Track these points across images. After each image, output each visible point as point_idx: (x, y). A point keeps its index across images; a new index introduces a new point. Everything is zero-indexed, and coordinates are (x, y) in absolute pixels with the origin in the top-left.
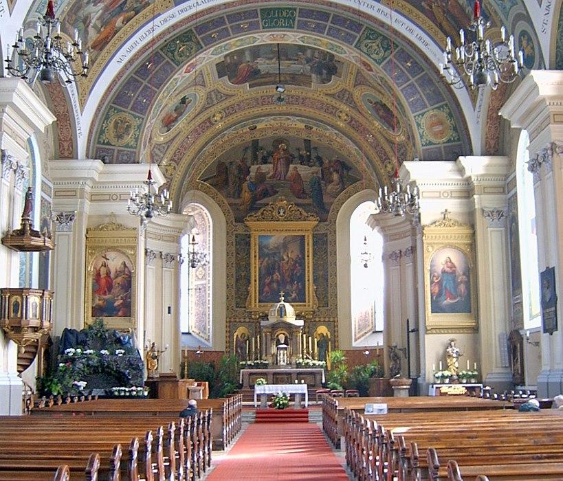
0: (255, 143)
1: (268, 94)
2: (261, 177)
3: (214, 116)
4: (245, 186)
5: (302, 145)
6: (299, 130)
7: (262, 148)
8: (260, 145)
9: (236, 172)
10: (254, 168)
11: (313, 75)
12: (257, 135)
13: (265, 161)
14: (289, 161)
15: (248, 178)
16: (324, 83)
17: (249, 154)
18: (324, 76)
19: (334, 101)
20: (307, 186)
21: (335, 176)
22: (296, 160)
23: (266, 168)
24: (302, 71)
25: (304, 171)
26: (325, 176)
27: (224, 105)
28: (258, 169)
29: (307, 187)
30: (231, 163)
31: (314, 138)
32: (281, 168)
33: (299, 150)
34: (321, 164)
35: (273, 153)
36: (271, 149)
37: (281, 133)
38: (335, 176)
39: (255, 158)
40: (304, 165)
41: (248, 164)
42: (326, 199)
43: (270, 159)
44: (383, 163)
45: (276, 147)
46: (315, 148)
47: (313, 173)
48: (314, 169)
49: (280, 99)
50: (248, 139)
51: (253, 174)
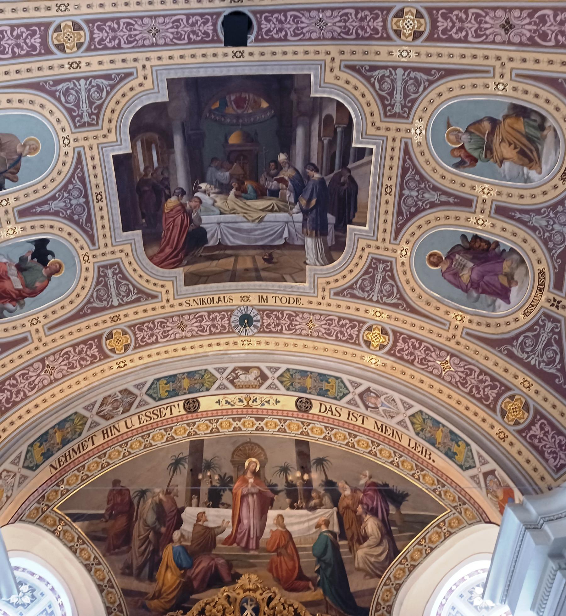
0: (197, 447)
1: (222, 306)
2: (206, 538)
3: (110, 336)
4: (168, 553)
5: (292, 458)
6: (283, 416)
7: (209, 466)
8: (207, 455)
9: (151, 517)
10: (190, 514)
11: (309, 242)
12: (202, 430)
13: (215, 500)
14: (265, 504)
15: (176, 535)
16: (331, 261)
17: (181, 480)
18: (330, 239)
19: (354, 304)
20: (309, 563)
21: (371, 525)
22: (282, 499)
23: (219, 517)
24: (286, 235)
25: (302, 524)
26: (348, 530)
27: (132, 314)
28: (201, 517)
29: (309, 563)
30: (142, 494)
31: (316, 436)
32: (249, 519)
33: (285, 470)
34: (336, 498)
35: (231, 480)
36: (228, 469)
37: (248, 428)
38: (371, 525)
39: (194, 490)
40: (298, 508)
41: (180, 503)
42: (356, 583)
43: (226, 497)
44: (494, 410)
45: (239, 466)
46: (320, 462)
47: (318, 526)
48: (323, 513)
49: (246, 320)
50: (182, 437)
51: (187, 527)
